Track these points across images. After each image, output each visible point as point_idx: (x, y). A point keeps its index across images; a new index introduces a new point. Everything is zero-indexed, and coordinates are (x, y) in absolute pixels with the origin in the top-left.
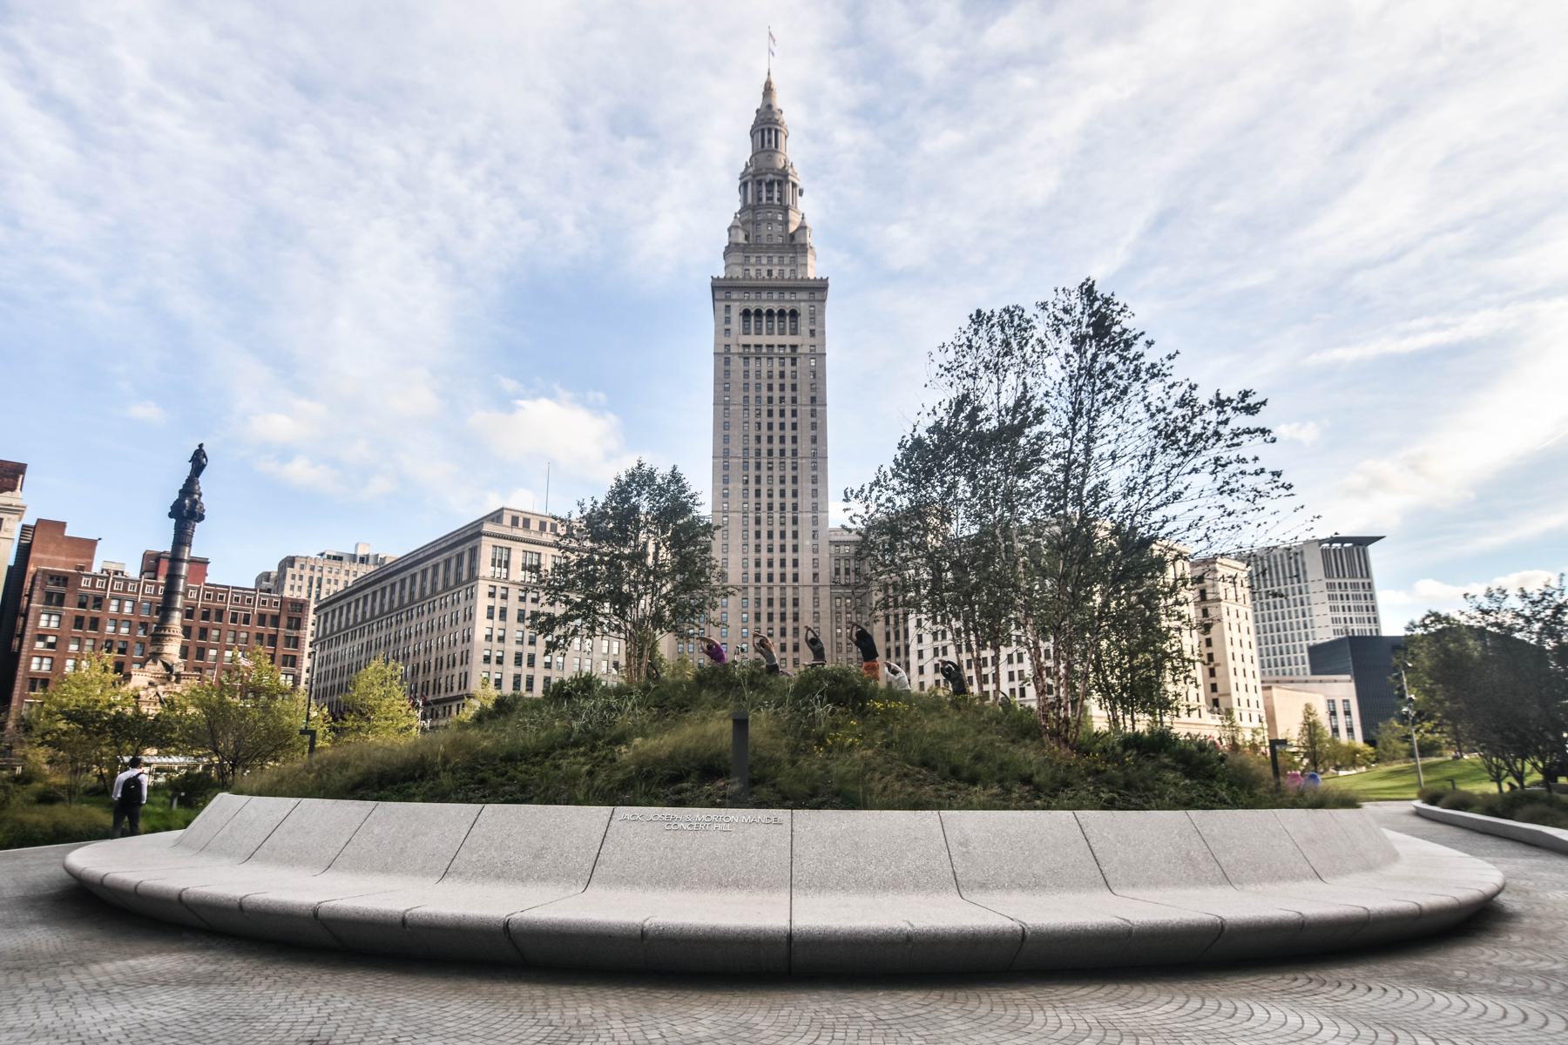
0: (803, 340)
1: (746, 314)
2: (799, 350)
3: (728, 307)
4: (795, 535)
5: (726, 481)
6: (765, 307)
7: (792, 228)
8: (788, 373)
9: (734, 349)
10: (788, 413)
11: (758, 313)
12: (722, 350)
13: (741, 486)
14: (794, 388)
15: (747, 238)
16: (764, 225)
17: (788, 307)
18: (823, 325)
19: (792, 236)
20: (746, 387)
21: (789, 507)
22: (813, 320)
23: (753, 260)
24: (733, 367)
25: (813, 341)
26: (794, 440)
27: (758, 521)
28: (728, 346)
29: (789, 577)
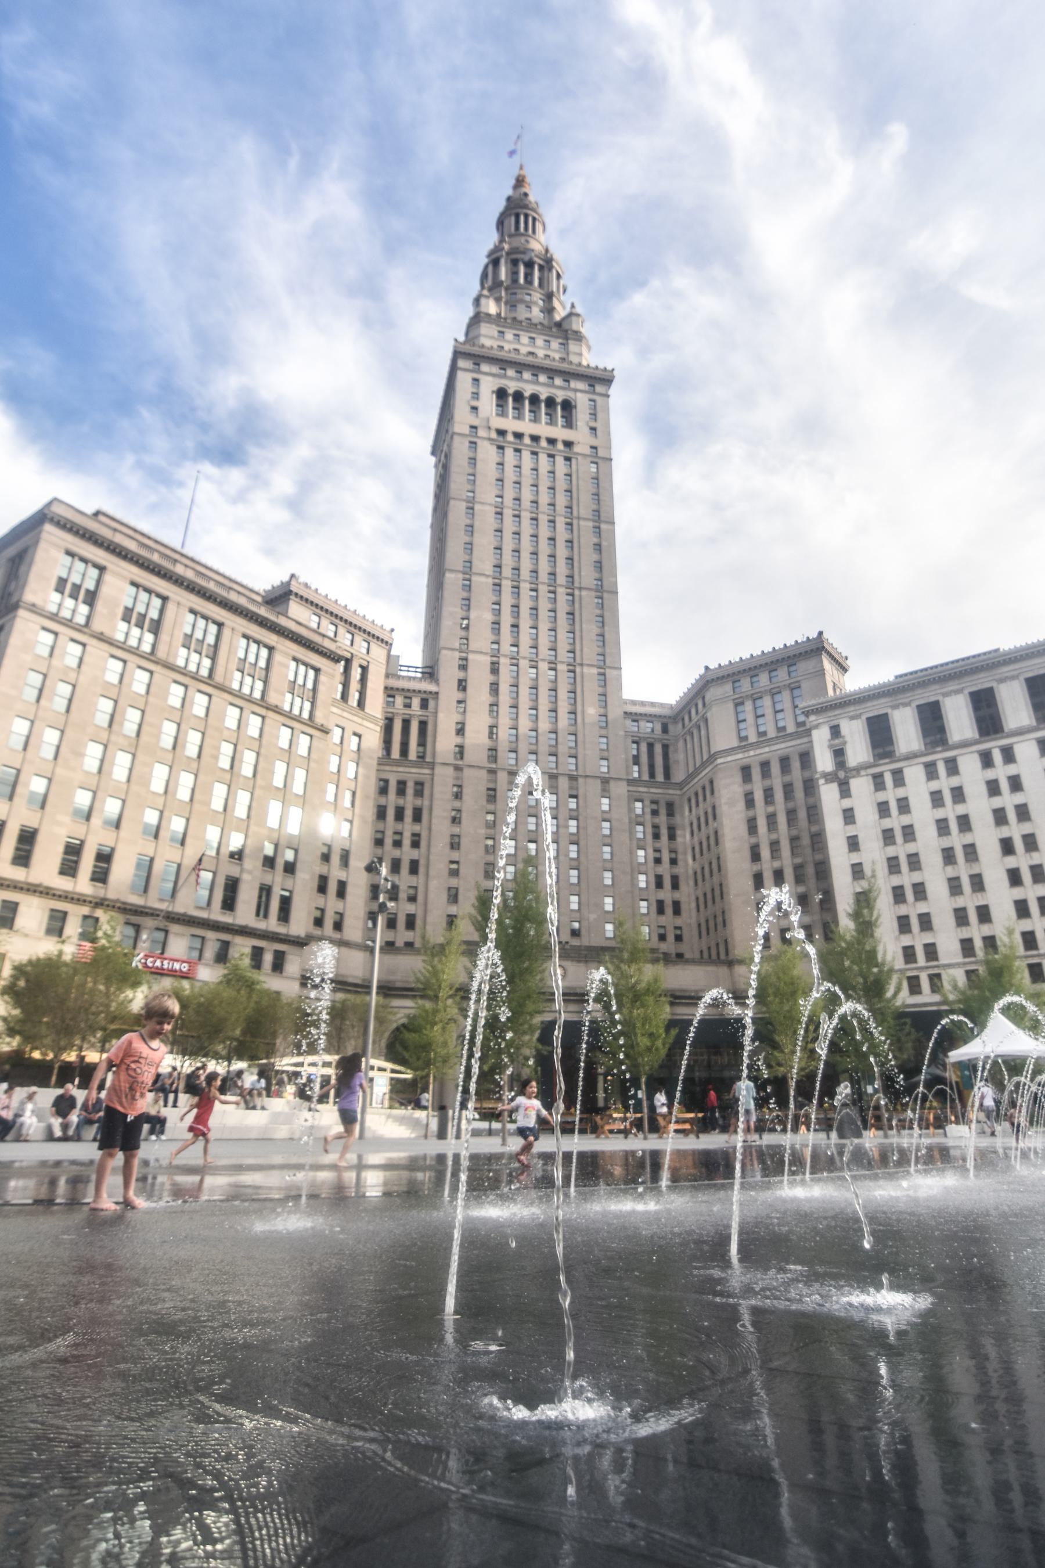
0: (580, 436)
2: (577, 449)
6: (528, 390)
7: (557, 318)
9: (482, 433)
11: (518, 396)
12: (466, 430)
13: (489, 617)
15: (499, 315)
16: (521, 308)
17: (560, 396)
19: (559, 325)
21: (563, 655)
23: (509, 335)
24: (480, 455)
25: (594, 443)
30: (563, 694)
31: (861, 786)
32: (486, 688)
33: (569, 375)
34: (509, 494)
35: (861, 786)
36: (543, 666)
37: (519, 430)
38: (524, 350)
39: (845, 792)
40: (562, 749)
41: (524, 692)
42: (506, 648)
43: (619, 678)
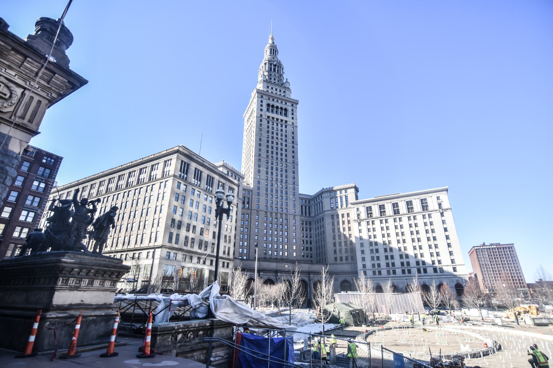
0: (289, 119)
1: (268, 105)
2: (288, 123)
3: (262, 101)
4: (286, 193)
5: (259, 167)
6: (276, 104)
8: (284, 130)
9: (263, 116)
10: (284, 145)
11: (273, 106)
13: (265, 169)
14: (286, 136)
16: (273, 79)
17: (284, 107)
18: (296, 116)
20: (268, 132)
21: (284, 181)
22: (293, 114)
23: (270, 88)
24: (263, 123)
26: (286, 156)
27: (272, 185)
28: (261, 116)
29: (285, 211)
30: (284, 192)
31: (364, 224)
32: (265, 189)
33: (287, 101)
34: (270, 135)
35: (364, 224)
36: (279, 184)
37: (273, 116)
38: (274, 92)
39: (359, 224)
40: (284, 207)
41: (274, 191)
42: (270, 179)
43: (298, 188)
